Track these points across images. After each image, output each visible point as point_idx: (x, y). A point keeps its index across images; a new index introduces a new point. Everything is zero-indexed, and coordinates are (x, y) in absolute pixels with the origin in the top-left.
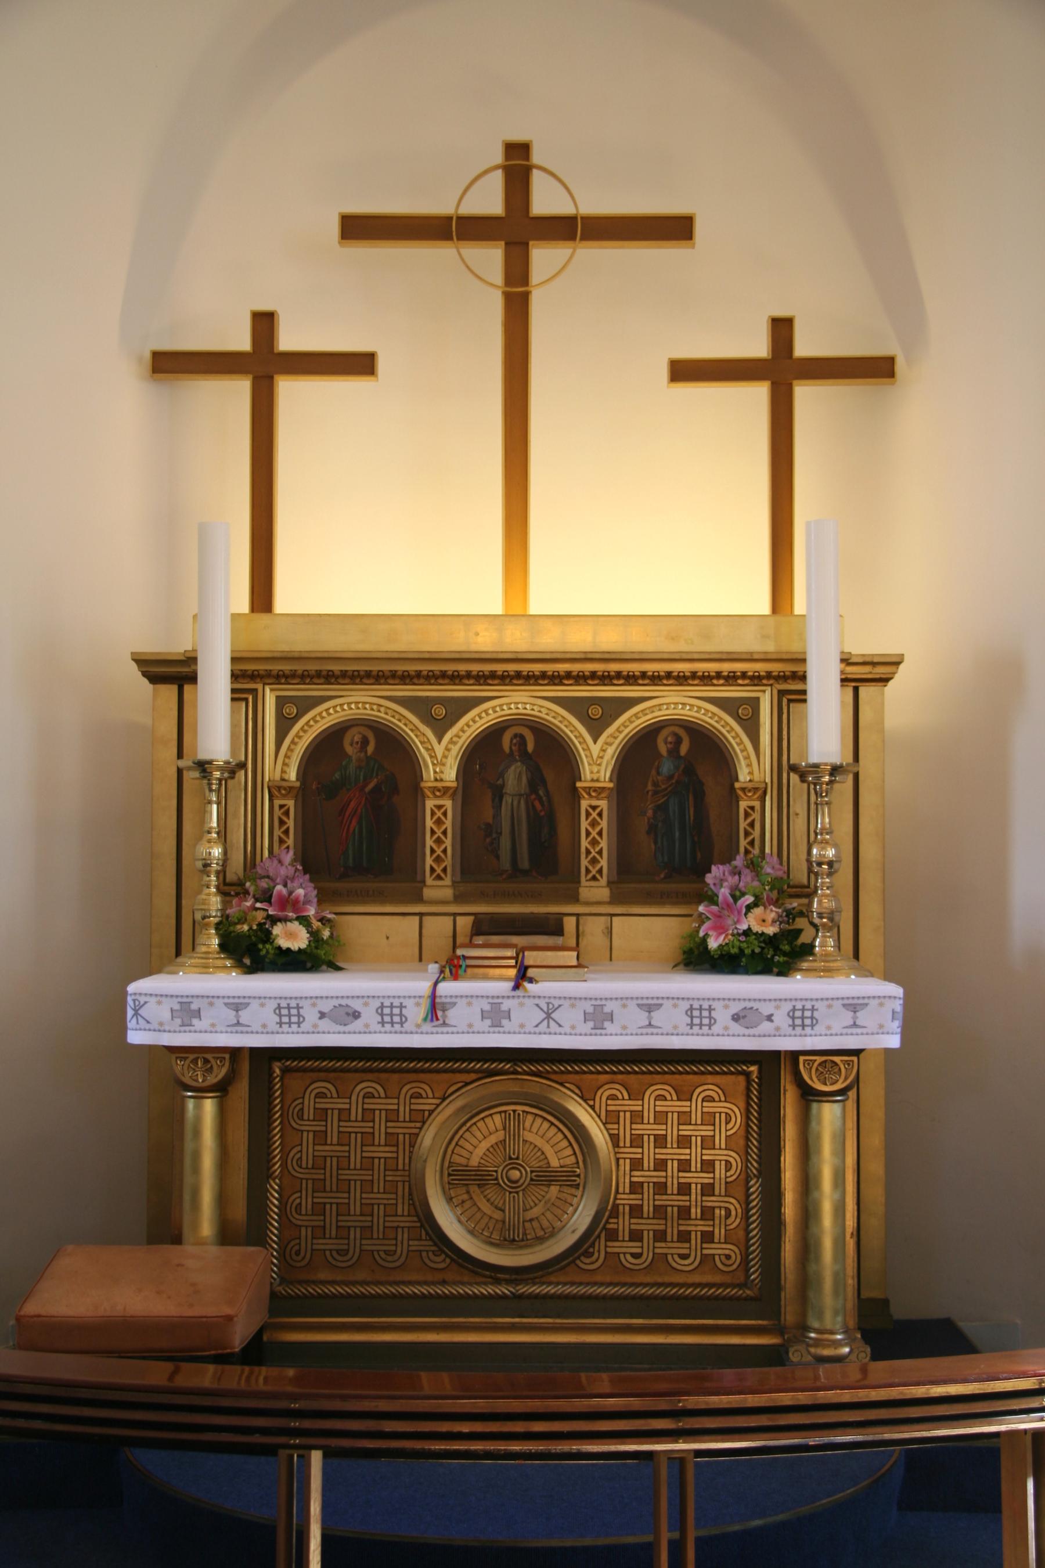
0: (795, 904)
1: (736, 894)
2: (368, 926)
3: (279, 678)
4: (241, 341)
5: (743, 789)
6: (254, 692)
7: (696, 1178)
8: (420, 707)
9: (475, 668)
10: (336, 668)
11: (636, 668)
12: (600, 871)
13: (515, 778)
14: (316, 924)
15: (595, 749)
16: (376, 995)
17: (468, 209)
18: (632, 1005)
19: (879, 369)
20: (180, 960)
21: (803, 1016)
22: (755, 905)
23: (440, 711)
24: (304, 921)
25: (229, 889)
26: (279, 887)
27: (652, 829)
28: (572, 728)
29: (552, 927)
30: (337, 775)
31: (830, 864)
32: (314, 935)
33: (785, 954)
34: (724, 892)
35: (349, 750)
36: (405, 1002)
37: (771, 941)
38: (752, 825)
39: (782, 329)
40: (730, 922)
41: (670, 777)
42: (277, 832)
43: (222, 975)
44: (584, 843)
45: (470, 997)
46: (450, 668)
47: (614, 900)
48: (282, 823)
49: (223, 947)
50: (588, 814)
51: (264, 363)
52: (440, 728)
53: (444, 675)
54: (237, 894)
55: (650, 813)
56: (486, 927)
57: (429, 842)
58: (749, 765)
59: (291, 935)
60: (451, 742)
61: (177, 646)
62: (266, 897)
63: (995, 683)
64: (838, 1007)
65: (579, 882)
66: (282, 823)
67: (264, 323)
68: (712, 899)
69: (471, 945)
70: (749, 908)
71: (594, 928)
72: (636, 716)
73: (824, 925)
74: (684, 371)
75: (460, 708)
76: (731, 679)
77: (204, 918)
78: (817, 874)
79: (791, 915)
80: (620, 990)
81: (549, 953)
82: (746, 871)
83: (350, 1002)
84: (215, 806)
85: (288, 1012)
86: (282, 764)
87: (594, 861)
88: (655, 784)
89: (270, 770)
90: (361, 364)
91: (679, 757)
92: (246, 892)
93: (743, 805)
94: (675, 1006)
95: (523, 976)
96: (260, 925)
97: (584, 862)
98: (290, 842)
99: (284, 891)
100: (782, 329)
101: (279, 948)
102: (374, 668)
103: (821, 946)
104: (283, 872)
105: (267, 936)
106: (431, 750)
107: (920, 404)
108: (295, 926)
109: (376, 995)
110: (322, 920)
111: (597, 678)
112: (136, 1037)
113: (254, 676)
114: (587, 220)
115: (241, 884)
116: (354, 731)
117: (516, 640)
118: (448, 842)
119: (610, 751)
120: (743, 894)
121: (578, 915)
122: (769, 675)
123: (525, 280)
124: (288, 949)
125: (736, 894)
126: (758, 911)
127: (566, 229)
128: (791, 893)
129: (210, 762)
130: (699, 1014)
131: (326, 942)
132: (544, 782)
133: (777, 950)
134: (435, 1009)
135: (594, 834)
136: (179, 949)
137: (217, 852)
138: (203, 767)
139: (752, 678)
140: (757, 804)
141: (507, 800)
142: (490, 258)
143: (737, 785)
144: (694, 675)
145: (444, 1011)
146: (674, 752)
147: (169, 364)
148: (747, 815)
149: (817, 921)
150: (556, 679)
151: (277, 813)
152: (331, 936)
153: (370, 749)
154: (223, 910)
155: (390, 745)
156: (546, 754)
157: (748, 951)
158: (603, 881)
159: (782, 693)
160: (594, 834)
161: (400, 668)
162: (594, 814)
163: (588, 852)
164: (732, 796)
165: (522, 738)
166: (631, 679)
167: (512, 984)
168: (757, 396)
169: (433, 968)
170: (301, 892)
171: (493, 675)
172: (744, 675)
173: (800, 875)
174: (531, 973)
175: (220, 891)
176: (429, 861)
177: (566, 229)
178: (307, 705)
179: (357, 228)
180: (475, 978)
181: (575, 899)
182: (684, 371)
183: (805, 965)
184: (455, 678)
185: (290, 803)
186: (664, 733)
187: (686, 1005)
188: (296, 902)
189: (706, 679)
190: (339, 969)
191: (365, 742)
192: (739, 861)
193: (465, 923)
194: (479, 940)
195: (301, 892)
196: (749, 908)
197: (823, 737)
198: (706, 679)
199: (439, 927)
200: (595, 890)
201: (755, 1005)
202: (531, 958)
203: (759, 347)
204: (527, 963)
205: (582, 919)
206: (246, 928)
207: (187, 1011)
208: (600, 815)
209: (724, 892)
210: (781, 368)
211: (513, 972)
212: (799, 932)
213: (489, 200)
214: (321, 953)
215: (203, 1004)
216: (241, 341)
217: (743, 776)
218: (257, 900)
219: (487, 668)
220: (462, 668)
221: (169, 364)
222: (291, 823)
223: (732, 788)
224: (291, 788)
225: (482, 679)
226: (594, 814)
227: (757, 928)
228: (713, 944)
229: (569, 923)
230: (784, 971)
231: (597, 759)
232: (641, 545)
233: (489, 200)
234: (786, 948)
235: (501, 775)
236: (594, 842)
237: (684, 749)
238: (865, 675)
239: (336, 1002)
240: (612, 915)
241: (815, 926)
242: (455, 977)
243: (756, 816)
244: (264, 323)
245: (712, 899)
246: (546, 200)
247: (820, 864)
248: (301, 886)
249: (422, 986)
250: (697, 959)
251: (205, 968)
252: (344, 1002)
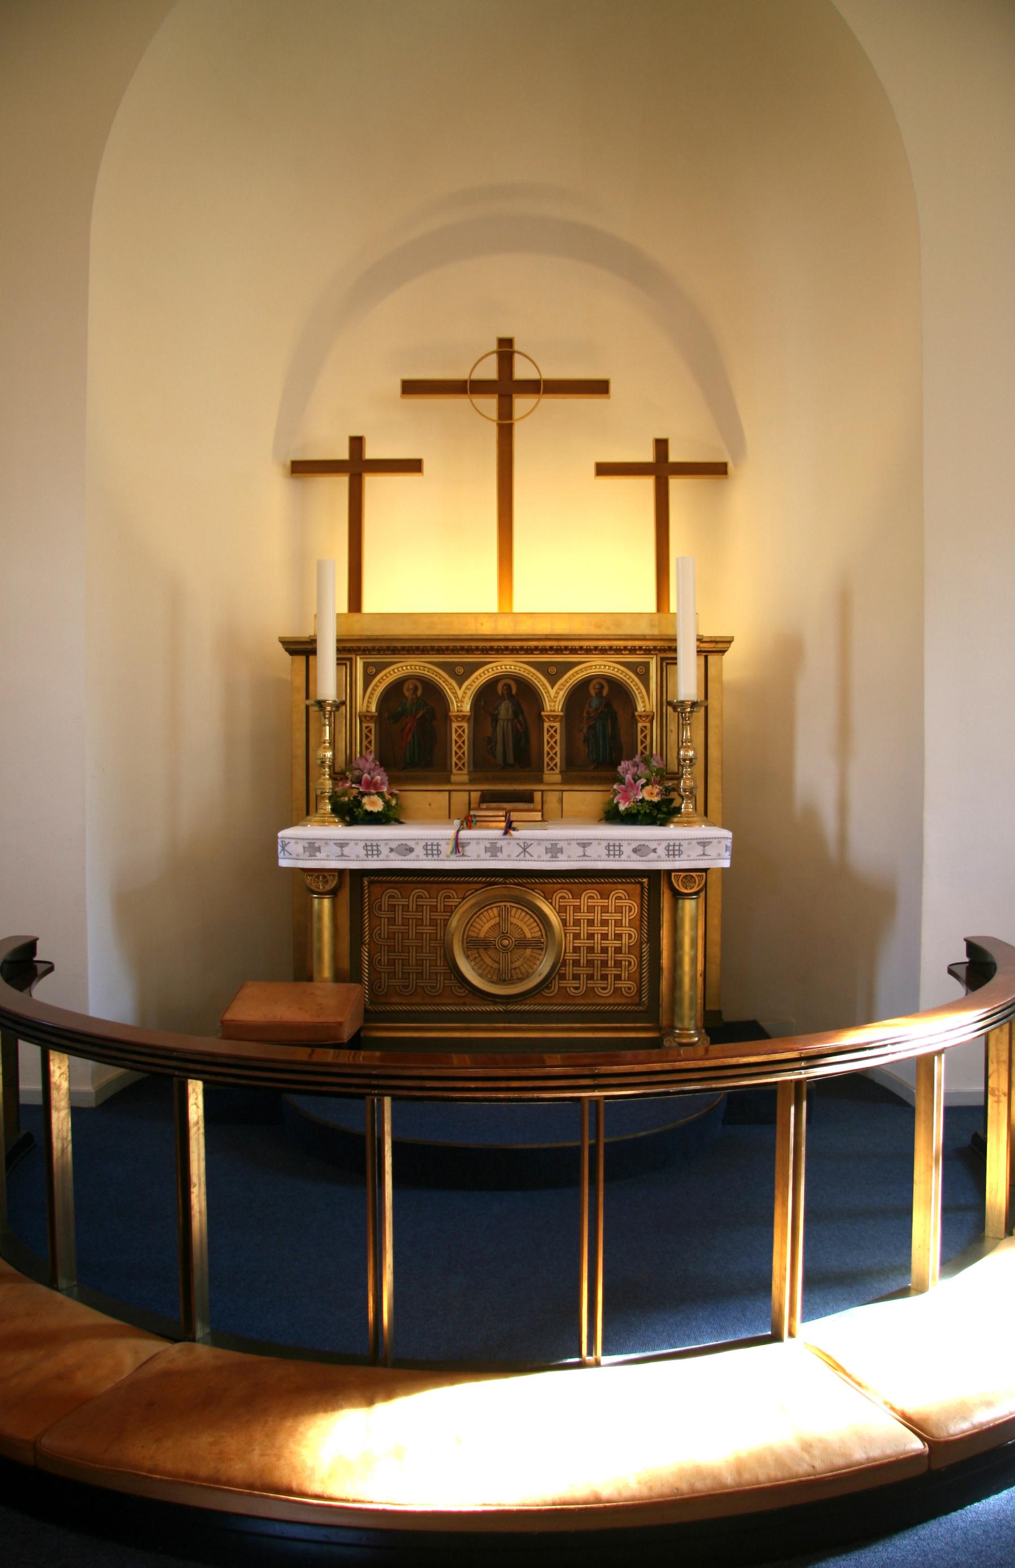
0: (670, 784)
1: (636, 778)
2: (419, 797)
3: (364, 651)
4: (343, 453)
5: (640, 716)
6: (350, 659)
7: (612, 944)
8: (449, 668)
9: (481, 644)
10: (399, 645)
11: (576, 644)
12: (556, 765)
13: (505, 710)
14: (388, 797)
15: (553, 692)
16: (423, 838)
17: (477, 375)
18: (574, 843)
19: (718, 470)
20: (309, 818)
21: (674, 849)
22: (647, 784)
23: (460, 670)
24: (381, 795)
25: (337, 776)
26: (366, 775)
27: (586, 740)
28: (539, 680)
29: (527, 798)
30: (400, 709)
31: (691, 760)
32: (387, 803)
33: (664, 813)
34: (628, 777)
35: (407, 694)
36: (440, 842)
37: (656, 806)
38: (645, 737)
39: (661, 446)
40: (632, 794)
41: (597, 709)
42: (365, 743)
43: (333, 827)
44: (546, 748)
45: (478, 840)
46: (466, 644)
47: (564, 782)
48: (367, 737)
49: (333, 810)
50: (548, 731)
51: (357, 466)
52: (461, 680)
53: (462, 649)
54: (341, 779)
55: (585, 730)
56: (488, 798)
57: (454, 748)
58: (644, 702)
59: (373, 803)
60: (467, 688)
61: (306, 633)
62: (358, 781)
63: (787, 655)
65: (543, 771)
66: (367, 737)
67: (357, 443)
68: (621, 781)
69: (479, 809)
70: (643, 786)
71: (552, 798)
72: (577, 673)
73: (687, 796)
74: (604, 470)
75: (472, 668)
76: (633, 650)
77: (322, 793)
78: (683, 766)
79: (668, 790)
80: (569, 835)
81: (525, 813)
82: (642, 765)
83: (408, 842)
84: (328, 728)
85: (372, 848)
86: (367, 702)
87: (552, 759)
88: (588, 713)
89: (360, 705)
90: (414, 466)
91: (602, 697)
92: (347, 778)
93: (640, 725)
94: (599, 844)
95: (509, 827)
96: (355, 797)
97: (546, 759)
98: (372, 748)
99: (369, 777)
100: (661, 446)
101: (366, 811)
102: (421, 644)
103: (686, 808)
104: (368, 766)
105: (359, 804)
106: (455, 693)
108: (375, 798)
109: (423, 838)
110: (392, 794)
111: (553, 650)
112: (283, 863)
113: (350, 650)
114: (546, 382)
115: (343, 773)
116: (410, 682)
117: (505, 628)
118: (465, 748)
119: (561, 693)
120: (640, 778)
121: (542, 791)
122: (655, 648)
123: (510, 416)
124: (372, 812)
125: (636, 778)
126: (649, 788)
127: (534, 387)
128: (668, 777)
129: (324, 701)
130: (614, 848)
131: (394, 807)
132: (522, 712)
133: (659, 811)
134: (458, 846)
135: (552, 743)
136: (307, 811)
137: (329, 754)
138: (321, 704)
139: (645, 650)
140: (648, 725)
141: (500, 723)
142: (490, 404)
143: (636, 714)
144: (611, 648)
145: (463, 847)
146: (599, 693)
147: (303, 468)
148: (642, 731)
149: (683, 793)
150: (529, 651)
151: (365, 731)
152: (397, 804)
153: (419, 693)
154: (333, 789)
155: (432, 692)
156: (522, 695)
157: (642, 812)
158: (557, 771)
159: (662, 659)
160: (552, 743)
161: (436, 644)
162: (552, 731)
163: (548, 754)
164: (634, 720)
165: (509, 685)
166: (573, 651)
167: (502, 832)
168: (647, 484)
169: (457, 822)
170: (379, 778)
171: (492, 649)
172: (640, 648)
173: (673, 767)
174: (514, 825)
175: (331, 777)
176: (454, 759)
177: (534, 387)
178: (381, 667)
179: (411, 388)
180: (481, 828)
181: (540, 781)
182: (604, 470)
183: (676, 820)
184: (469, 651)
185: (372, 725)
186: (594, 682)
187: (605, 844)
188: (376, 784)
189: (618, 651)
190: (401, 823)
191: (416, 689)
192: (637, 759)
193: (475, 796)
194: (484, 806)
195: (379, 778)
196: (643, 786)
197: (687, 685)
198: (618, 651)
199: (460, 799)
200: (552, 776)
201: (646, 843)
202: (514, 816)
203: (647, 456)
204: (512, 819)
205: (545, 793)
206: (346, 799)
207: (313, 847)
208: (555, 731)
209: (628, 777)
210: (661, 469)
211: (503, 825)
212: (672, 800)
213: (489, 371)
214: (391, 813)
215: (321, 844)
216: (343, 453)
217: (640, 708)
218: (353, 783)
219: (488, 644)
220: (473, 644)
221: (303, 468)
222: (372, 737)
223: (633, 717)
224: (372, 717)
225: (485, 651)
226: (552, 731)
227: (647, 798)
228: (622, 807)
229: (538, 796)
230: (663, 823)
231: (554, 698)
232: (580, 569)
233: (489, 371)
234: (665, 809)
235: (497, 708)
236: (552, 748)
237: (605, 692)
238: (711, 649)
239: (399, 843)
240: (563, 791)
241: (682, 797)
242: (470, 828)
243: (648, 732)
244: (357, 443)
245: (621, 781)
246: (522, 371)
247: (685, 760)
248: (379, 774)
249: (451, 833)
250: (612, 816)
251: (323, 823)
252: (404, 842)
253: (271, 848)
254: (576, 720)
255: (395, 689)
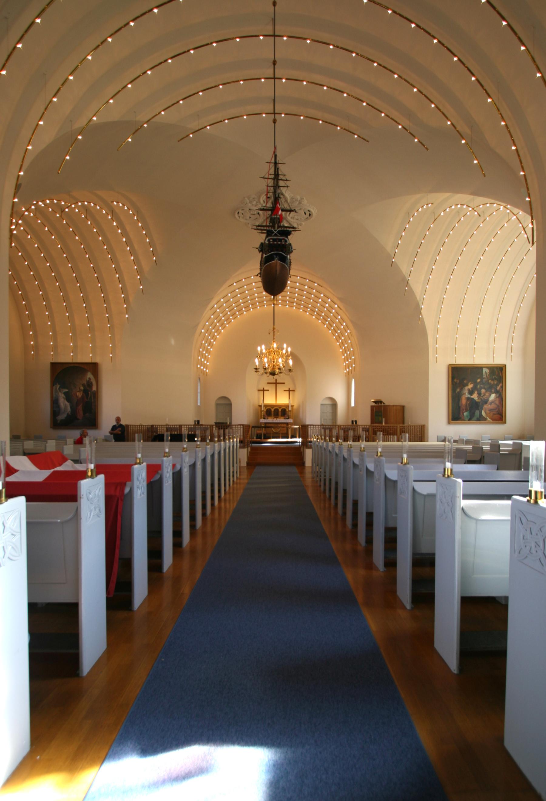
2: (269, 418)
16: (270, 420)
19: (294, 391)
51: (264, 390)
64: (290, 421)
74: (285, 391)
80: (281, 420)
86: (265, 410)
90: (268, 390)
107: (296, 393)
109: (270, 420)
111: (280, 406)
147: (259, 390)
179: (268, 383)
197: (290, 409)
210: (289, 391)
215: (262, 421)
221: (259, 390)
231: (280, 410)
232: (283, 400)
238: (292, 406)
253: (259, 421)
254: (281, 411)
255: (267, 410)
